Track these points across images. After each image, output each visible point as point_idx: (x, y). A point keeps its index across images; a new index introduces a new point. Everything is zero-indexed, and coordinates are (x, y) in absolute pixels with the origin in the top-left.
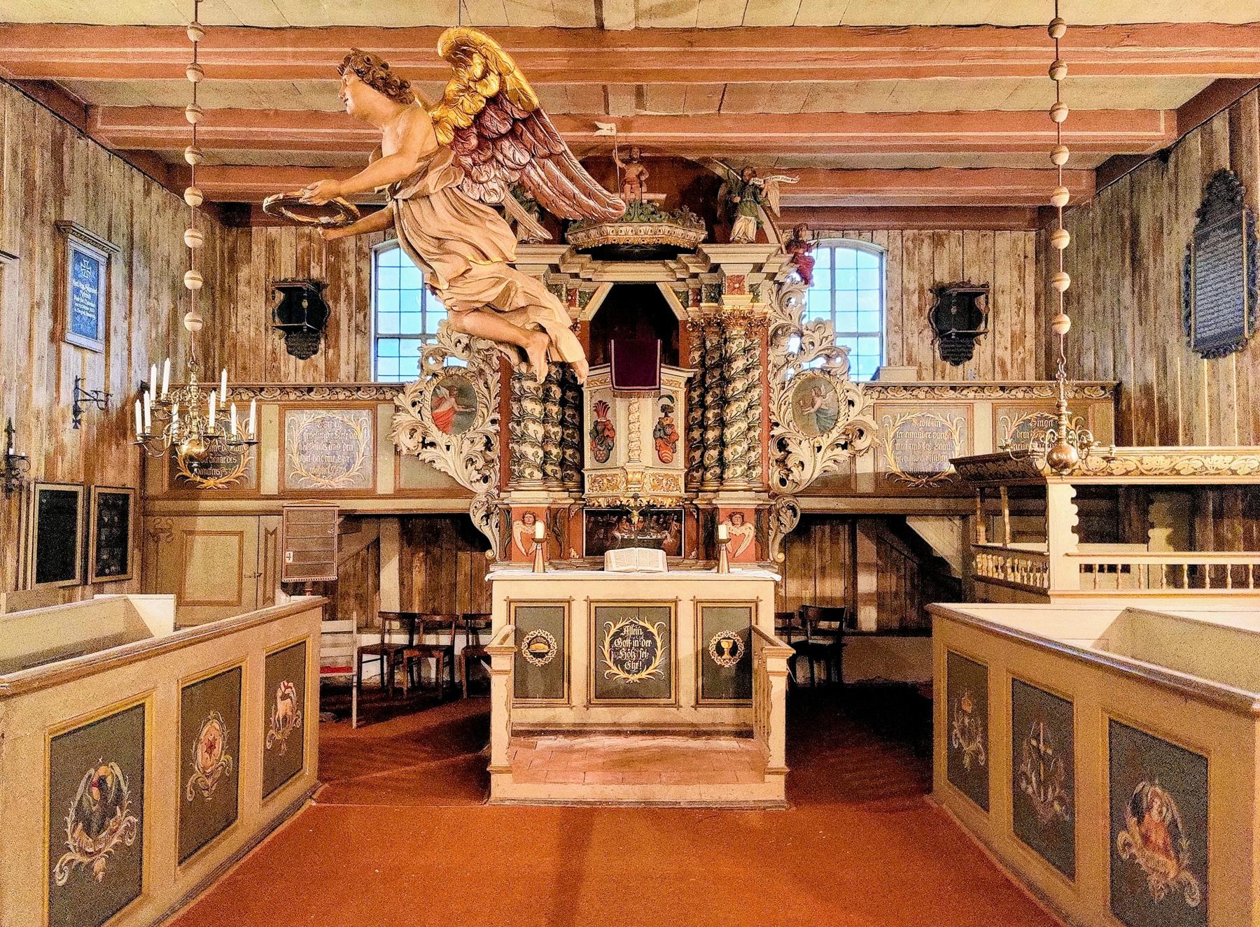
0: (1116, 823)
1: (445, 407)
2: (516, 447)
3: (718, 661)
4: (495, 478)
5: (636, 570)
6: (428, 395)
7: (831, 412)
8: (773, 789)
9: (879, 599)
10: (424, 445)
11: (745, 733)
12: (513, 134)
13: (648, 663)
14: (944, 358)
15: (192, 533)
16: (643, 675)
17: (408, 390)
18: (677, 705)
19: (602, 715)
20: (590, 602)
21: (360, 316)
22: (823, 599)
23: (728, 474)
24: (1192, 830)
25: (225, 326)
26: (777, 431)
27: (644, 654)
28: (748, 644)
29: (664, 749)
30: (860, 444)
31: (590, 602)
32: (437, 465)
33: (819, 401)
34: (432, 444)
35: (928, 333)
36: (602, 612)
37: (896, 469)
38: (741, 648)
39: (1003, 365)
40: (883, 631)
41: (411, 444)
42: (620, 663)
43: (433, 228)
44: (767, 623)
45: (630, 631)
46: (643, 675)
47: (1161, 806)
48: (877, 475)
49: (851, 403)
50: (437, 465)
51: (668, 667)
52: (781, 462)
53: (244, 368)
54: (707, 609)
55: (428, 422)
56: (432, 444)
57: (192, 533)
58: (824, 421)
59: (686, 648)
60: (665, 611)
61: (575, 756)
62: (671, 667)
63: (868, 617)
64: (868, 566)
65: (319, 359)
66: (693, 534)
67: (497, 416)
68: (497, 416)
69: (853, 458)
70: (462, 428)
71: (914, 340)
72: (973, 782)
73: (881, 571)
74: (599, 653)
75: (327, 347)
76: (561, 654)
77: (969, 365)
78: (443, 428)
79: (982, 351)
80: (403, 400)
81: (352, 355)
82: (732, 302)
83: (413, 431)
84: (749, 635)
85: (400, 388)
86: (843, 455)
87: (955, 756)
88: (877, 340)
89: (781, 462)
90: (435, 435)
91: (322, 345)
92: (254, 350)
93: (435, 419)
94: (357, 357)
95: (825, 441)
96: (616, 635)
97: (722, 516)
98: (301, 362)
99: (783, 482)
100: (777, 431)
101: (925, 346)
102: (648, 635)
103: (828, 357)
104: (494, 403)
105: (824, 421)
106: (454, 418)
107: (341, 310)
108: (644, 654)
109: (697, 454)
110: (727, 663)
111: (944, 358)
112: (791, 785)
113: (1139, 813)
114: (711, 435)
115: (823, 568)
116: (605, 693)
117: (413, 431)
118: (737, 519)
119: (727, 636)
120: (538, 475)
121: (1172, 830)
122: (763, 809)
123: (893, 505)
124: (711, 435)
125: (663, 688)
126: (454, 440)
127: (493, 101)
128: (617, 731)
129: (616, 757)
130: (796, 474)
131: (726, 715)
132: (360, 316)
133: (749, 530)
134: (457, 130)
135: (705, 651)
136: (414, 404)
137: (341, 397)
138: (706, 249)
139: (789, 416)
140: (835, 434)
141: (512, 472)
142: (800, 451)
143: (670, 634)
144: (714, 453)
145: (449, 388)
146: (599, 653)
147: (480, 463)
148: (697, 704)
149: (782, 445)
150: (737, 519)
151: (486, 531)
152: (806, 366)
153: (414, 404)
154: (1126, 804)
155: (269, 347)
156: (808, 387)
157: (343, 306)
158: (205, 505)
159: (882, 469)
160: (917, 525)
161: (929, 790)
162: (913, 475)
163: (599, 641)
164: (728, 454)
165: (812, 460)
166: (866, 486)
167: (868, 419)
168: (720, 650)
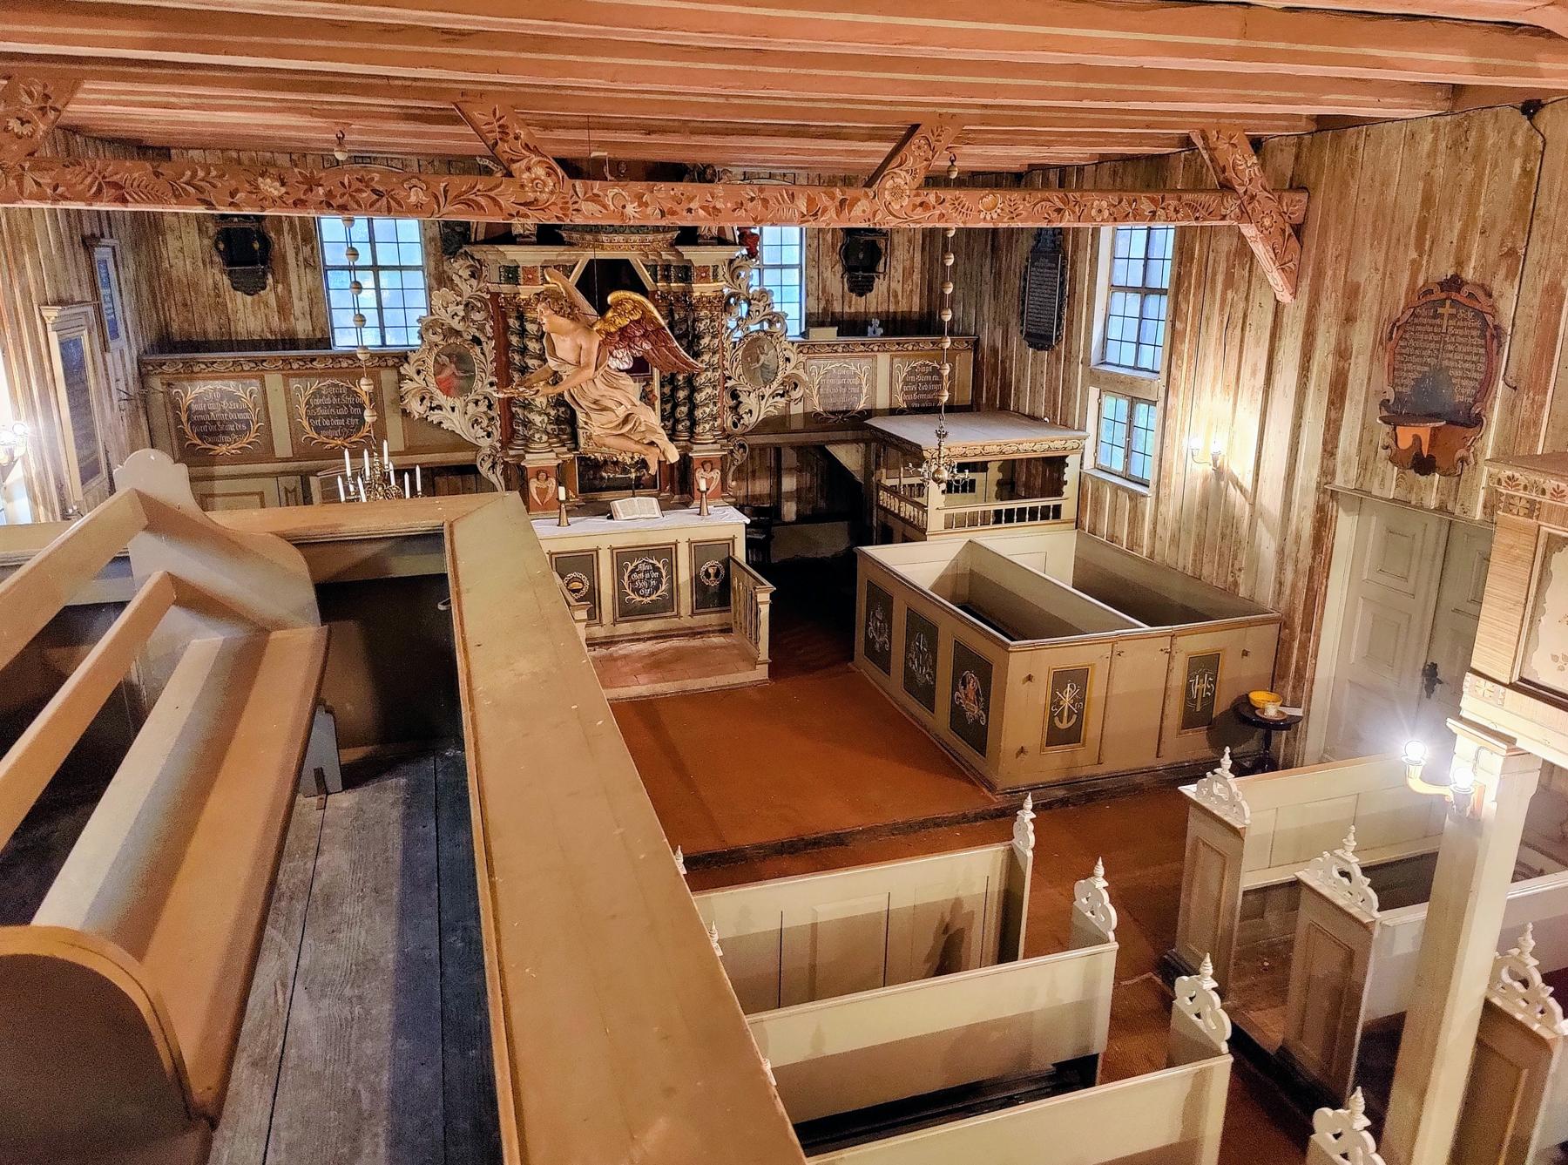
0: (955, 688)
1: (447, 372)
2: (519, 411)
3: (706, 582)
4: (497, 434)
5: (638, 518)
6: (431, 362)
7: (772, 366)
8: (762, 673)
9: (798, 495)
10: (432, 409)
11: (726, 630)
12: (645, 336)
13: (657, 588)
14: (851, 290)
15: (212, 495)
16: (654, 597)
17: (413, 357)
18: (678, 616)
19: (625, 628)
20: (612, 549)
21: (307, 250)
22: (754, 497)
23: (699, 429)
24: (984, 694)
25: (158, 259)
26: (730, 384)
27: (653, 583)
28: (727, 569)
29: (676, 649)
30: (796, 394)
31: (612, 549)
32: (444, 426)
33: (762, 358)
34: (439, 407)
35: (839, 268)
36: (622, 557)
37: (819, 409)
38: (723, 572)
39: (896, 296)
40: (801, 518)
41: (421, 409)
42: (636, 591)
43: (595, 395)
44: (740, 553)
45: (643, 567)
46: (654, 597)
47: (973, 683)
48: (806, 414)
49: (788, 360)
50: (444, 426)
51: (671, 590)
52: (735, 409)
53: (185, 305)
54: (700, 549)
55: (433, 387)
56: (439, 407)
57: (212, 495)
58: (767, 375)
59: (684, 575)
60: (667, 552)
61: (619, 663)
62: (673, 590)
63: (790, 510)
64: (790, 470)
65: (269, 295)
66: (677, 485)
67: (495, 379)
68: (495, 379)
69: (788, 404)
70: (464, 391)
71: (828, 274)
72: (881, 659)
73: (800, 470)
74: (621, 586)
75: (276, 282)
76: (592, 588)
77: (871, 296)
78: (447, 393)
79: (880, 285)
80: (407, 369)
81: (305, 290)
82: (700, 289)
83: (422, 399)
84: (728, 562)
85: (403, 358)
86: (781, 402)
87: (869, 642)
88: (797, 271)
89: (735, 409)
90: (441, 399)
91: (270, 280)
92: (193, 286)
93: (439, 383)
94: (310, 292)
95: (767, 391)
96: (633, 571)
97: (696, 464)
98: (249, 298)
99: (735, 425)
100: (730, 384)
101: (835, 281)
102: (656, 569)
103: (771, 323)
104: (491, 367)
105: (767, 375)
106: (456, 382)
107: (287, 244)
108: (653, 583)
109: (668, 407)
110: (713, 583)
111: (851, 290)
112: (774, 670)
113: (964, 684)
114: (682, 394)
115: (754, 472)
116: (626, 611)
117: (422, 399)
118: (708, 466)
119: (711, 566)
120: (545, 438)
121: (977, 693)
122: (754, 686)
123: (817, 437)
124: (682, 394)
125: (666, 605)
126: (459, 403)
127: (638, 322)
128: (636, 638)
129: (647, 661)
130: (746, 419)
131: (712, 618)
132: (307, 250)
133: (716, 474)
134: (608, 334)
135: (697, 576)
136: (418, 372)
137: (344, 365)
138: (680, 248)
139: (740, 370)
140: (775, 386)
141: (514, 431)
142: (749, 401)
143: (672, 567)
144: (684, 409)
145: (449, 356)
146: (621, 586)
147: (485, 423)
148: (693, 614)
149: (734, 395)
150: (708, 466)
151: (493, 479)
152: (754, 328)
153: (418, 372)
154: (958, 680)
155: (210, 281)
156: (753, 346)
157: (287, 238)
158: (220, 470)
159: (809, 410)
160: (830, 448)
161: (852, 659)
162: (833, 413)
163: (620, 575)
164: (699, 413)
165: (757, 407)
166: (797, 424)
167: (801, 372)
168: (707, 574)
